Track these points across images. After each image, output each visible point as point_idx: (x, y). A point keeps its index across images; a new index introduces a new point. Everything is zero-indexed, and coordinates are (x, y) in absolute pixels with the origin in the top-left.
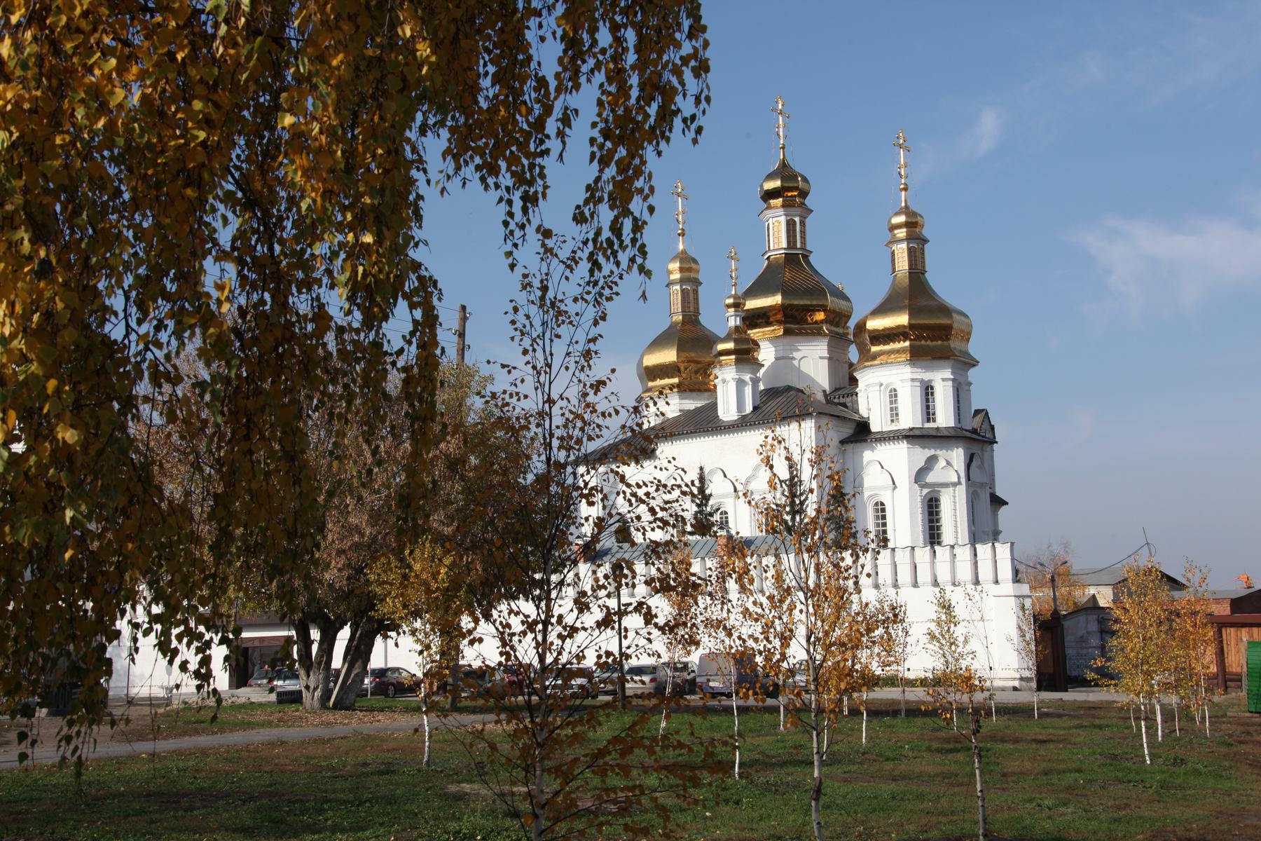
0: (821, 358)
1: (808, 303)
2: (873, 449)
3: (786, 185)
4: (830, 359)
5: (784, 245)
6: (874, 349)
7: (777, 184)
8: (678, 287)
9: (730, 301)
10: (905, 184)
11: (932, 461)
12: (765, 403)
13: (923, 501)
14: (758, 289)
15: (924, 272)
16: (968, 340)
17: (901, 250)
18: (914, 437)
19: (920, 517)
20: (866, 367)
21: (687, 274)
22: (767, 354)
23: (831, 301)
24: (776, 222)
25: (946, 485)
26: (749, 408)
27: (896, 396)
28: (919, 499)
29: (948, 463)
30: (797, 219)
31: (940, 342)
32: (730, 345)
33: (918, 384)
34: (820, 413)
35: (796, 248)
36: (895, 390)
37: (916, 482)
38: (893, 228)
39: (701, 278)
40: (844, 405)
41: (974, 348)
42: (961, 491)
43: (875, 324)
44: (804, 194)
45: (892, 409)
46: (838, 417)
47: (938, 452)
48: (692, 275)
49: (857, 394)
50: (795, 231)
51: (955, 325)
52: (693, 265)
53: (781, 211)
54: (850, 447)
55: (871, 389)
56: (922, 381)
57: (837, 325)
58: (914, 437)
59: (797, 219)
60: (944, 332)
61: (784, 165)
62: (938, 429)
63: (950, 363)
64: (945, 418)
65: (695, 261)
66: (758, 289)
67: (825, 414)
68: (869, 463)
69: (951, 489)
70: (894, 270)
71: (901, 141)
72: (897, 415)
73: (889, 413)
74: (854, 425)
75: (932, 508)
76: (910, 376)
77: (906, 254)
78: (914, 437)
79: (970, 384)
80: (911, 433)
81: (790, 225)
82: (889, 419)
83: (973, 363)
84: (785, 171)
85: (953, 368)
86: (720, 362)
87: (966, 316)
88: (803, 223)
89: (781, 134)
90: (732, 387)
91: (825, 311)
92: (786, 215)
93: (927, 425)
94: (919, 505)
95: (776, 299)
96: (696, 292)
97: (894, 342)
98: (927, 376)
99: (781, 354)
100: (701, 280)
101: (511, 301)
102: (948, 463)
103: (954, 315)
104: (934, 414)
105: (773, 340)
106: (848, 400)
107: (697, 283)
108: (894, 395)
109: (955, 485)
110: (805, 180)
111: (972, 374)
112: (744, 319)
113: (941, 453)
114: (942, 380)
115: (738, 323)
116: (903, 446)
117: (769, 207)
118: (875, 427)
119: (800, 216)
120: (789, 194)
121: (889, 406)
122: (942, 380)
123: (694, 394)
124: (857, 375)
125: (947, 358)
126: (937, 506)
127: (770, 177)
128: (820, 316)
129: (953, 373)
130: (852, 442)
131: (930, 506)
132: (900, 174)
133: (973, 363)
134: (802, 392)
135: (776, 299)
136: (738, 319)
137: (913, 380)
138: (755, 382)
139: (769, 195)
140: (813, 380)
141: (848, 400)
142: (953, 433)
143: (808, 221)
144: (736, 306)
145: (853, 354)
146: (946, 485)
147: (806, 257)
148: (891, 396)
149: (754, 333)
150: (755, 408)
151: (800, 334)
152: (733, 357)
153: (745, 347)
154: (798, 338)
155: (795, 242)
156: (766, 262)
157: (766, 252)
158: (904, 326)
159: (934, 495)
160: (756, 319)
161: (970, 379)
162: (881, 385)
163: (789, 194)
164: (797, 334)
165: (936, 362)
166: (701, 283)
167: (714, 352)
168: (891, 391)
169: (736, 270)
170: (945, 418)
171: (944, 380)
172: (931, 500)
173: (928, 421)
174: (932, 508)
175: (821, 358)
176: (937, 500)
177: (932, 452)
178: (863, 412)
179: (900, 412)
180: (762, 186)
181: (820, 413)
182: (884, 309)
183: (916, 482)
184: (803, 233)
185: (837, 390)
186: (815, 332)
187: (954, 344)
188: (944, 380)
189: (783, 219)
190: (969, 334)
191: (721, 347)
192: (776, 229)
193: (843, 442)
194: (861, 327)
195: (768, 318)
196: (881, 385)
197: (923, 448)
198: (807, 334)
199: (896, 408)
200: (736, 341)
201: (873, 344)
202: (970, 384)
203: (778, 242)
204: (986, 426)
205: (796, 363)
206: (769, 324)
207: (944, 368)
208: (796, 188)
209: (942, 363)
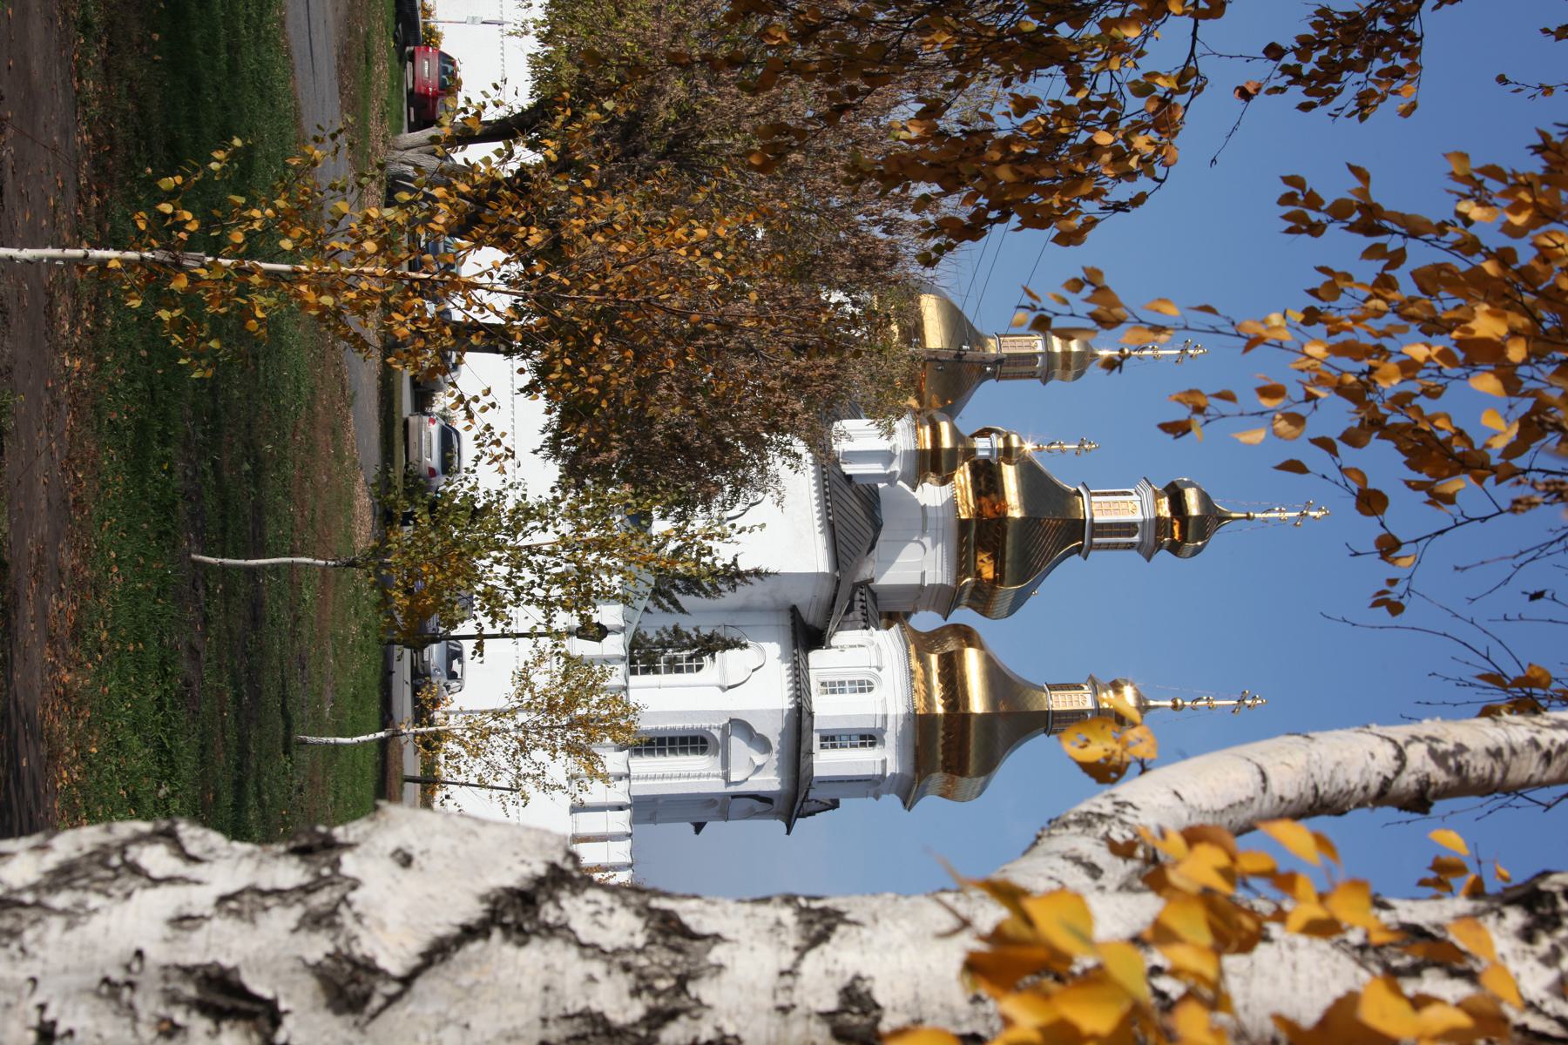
0: (923, 574)
1: (1008, 558)
2: (783, 658)
3: (1191, 523)
4: (921, 587)
5: (1098, 519)
6: (934, 659)
7: (1194, 508)
8: (1040, 348)
9: (1015, 443)
10: (1183, 706)
11: (763, 744)
12: (857, 492)
13: (701, 729)
14: (1033, 478)
15: (1048, 732)
16: (942, 795)
17: (1082, 700)
18: (799, 720)
19: (679, 725)
20: (907, 647)
21: (1059, 363)
22: (931, 494)
23: (1009, 590)
25: (725, 764)
26: (849, 469)
27: (862, 691)
28: (705, 725)
29: (758, 769)
30: (1136, 538)
31: (941, 757)
32: (946, 442)
33: (879, 725)
34: (838, 582)
35: (1093, 535)
36: (870, 690)
37: (731, 721)
38: (1116, 686)
39: (1054, 384)
40: (850, 609)
41: (931, 804)
42: (716, 786)
43: (972, 662)
44: (1175, 548)
45: (842, 683)
46: (832, 606)
47: (775, 756)
48: (1058, 371)
49: (866, 628)
50: (1119, 535)
51: (965, 780)
52: (1073, 372)
53: (1150, 515)
54: (786, 620)
55: (873, 653)
56: (883, 730)
57: (972, 596)
58: (800, 719)
59: (1136, 538)
60: (956, 765)
61: (1221, 518)
62: (811, 753)
63: (910, 772)
64: (827, 762)
65: (1078, 375)
66: (1033, 478)
67: (837, 590)
68: (762, 649)
69: (719, 771)
70: (1053, 687)
71: (1248, 702)
72: (833, 692)
73: (836, 679)
74: (819, 625)
75: (693, 742)
76: (891, 712)
77: (1075, 707)
78: (800, 719)
79: (877, 797)
80: (805, 715)
81: (1128, 528)
82: (828, 679)
83: (908, 801)
84: (1212, 518)
85: (901, 775)
86: (922, 426)
87: (980, 794)
88: (1131, 546)
89: (1270, 515)
90: (883, 444)
91: (994, 581)
92: (1144, 522)
93: (816, 737)
94: (697, 725)
95: (1015, 512)
96: (1032, 375)
97: (943, 689)
98: (890, 738)
99: (930, 514)
100: (1050, 383)
101: (1358, 172)
102: (758, 769)
103: (982, 779)
104: (834, 746)
105: (953, 504)
106: (857, 614)
107: (1046, 377)
108: (864, 687)
109: (726, 777)
110: (1197, 551)
111: (892, 801)
112: (987, 461)
113: (772, 760)
114: (885, 759)
115: (980, 453)
116: (785, 702)
117: (1157, 495)
118: (816, 658)
119: (1142, 543)
120: (1176, 528)
121: (847, 679)
122: (885, 759)
124: (895, 629)
125: (917, 768)
126: (695, 751)
127: (1205, 499)
128: (988, 572)
129: (893, 775)
130: (793, 624)
131: (694, 739)
132: (1199, 699)
133: (908, 801)
134: (872, 547)
135: (1015, 512)
136: (987, 453)
137: (885, 717)
138: (890, 479)
139: (1175, 495)
140: (892, 562)
141: (857, 614)
142: (803, 775)
143: (1134, 553)
144: (1007, 453)
145: (925, 621)
146: (725, 764)
147: (1079, 550)
148: (861, 683)
149: (963, 476)
150: (849, 478)
151: (960, 544)
152: (928, 446)
153: (944, 464)
155: (1101, 535)
156: (1073, 489)
157: (1087, 489)
158: (966, 705)
159: (711, 746)
160: (986, 478)
161: (884, 797)
162: (879, 669)
163: (1176, 528)
164: (960, 540)
165: (910, 752)
166: (1044, 383)
167: (937, 415)
168: (869, 683)
169: (1063, 451)
170: (827, 762)
171: (884, 762)
172: (704, 741)
173: (824, 739)
174: (693, 742)
175: (923, 574)
176: (703, 750)
177: (775, 746)
178: (841, 638)
179: (837, 697)
180: (1190, 484)
181: (838, 582)
182: (996, 677)
183: (731, 721)
184: (1116, 546)
185: (874, 595)
186: (963, 564)
187: (938, 778)
188: (884, 762)
189: (1137, 517)
190: (953, 798)
191: (945, 427)
192: (1124, 506)
193: (794, 610)
194: (967, 636)
195: (986, 495)
196: (879, 669)
197: (782, 734)
198: (960, 554)
199: (843, 691)
200: (953, 451)
201: (941, 658)
202: (877, 797)
203: (1100, 509)
204: (813, 806)
206: (978, 494)
207: (902, 761)
208: (1184, 537)
209: (910, 760)
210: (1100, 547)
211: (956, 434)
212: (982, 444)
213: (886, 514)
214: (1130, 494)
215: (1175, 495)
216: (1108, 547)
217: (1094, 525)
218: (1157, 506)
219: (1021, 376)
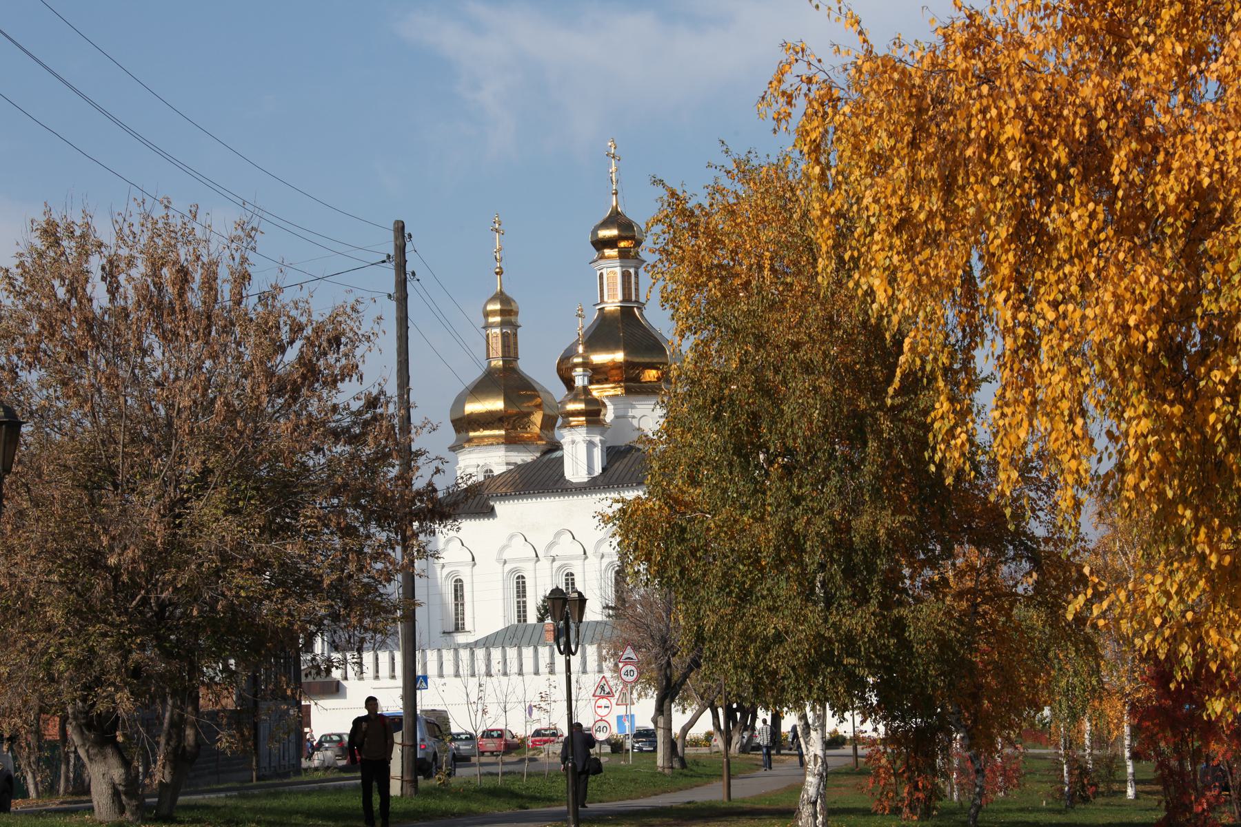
3: (623, 234)
5: (620, 297)
7: (613, 232)
8: (498, 331)
21: (507, 318)
22: (609, 415)
24: (612, 270)
26: (598, 470)
30: (632, 271)
35: (630, 301)
50: (630, 283)
53: (617, 262)
59: (632, 271)
81: (626, 276)
88: (636, 274)
90: (582, 449)
92: (621, 266)
95: (619, 356)
96: (515, 335)
99: (621, 413)
117: (602, 257)
123: (515, 446)
127: (606, 224)
135: (619, 356)
136: (586, 378)
139: (600, 244)
149: (597, 391)
150: (604, 469)
153: (596, 408)
154: (640, 397)
160: (599, 374)
184: (637, 283)
189: (618, 270)
205: (635, 422)
206: (606, 381)
208: (632, 238)
210: (637, 295)
211: (575, 399)
212: (580, 382)
213: (622, 442)
214: (601, 275)
215: (600, 244)
216: (637, 290)
217: (624, 301)
218: (609, 258)
219: (516, 344)
